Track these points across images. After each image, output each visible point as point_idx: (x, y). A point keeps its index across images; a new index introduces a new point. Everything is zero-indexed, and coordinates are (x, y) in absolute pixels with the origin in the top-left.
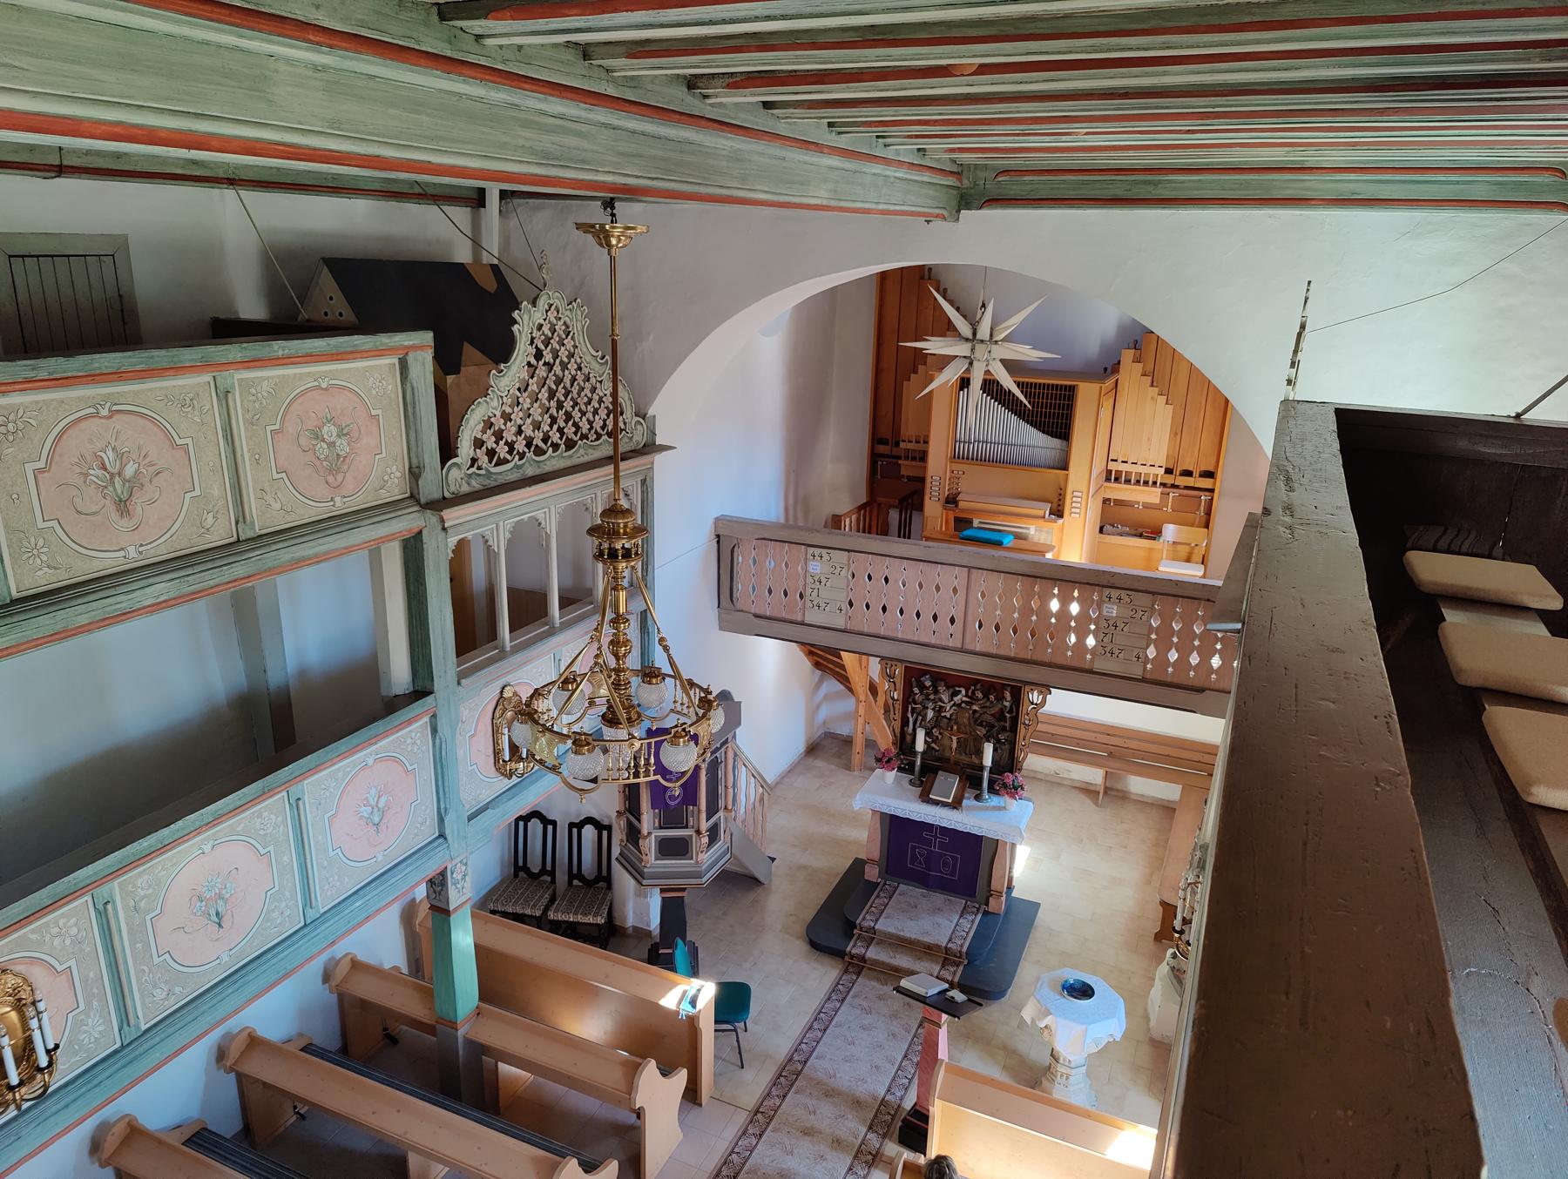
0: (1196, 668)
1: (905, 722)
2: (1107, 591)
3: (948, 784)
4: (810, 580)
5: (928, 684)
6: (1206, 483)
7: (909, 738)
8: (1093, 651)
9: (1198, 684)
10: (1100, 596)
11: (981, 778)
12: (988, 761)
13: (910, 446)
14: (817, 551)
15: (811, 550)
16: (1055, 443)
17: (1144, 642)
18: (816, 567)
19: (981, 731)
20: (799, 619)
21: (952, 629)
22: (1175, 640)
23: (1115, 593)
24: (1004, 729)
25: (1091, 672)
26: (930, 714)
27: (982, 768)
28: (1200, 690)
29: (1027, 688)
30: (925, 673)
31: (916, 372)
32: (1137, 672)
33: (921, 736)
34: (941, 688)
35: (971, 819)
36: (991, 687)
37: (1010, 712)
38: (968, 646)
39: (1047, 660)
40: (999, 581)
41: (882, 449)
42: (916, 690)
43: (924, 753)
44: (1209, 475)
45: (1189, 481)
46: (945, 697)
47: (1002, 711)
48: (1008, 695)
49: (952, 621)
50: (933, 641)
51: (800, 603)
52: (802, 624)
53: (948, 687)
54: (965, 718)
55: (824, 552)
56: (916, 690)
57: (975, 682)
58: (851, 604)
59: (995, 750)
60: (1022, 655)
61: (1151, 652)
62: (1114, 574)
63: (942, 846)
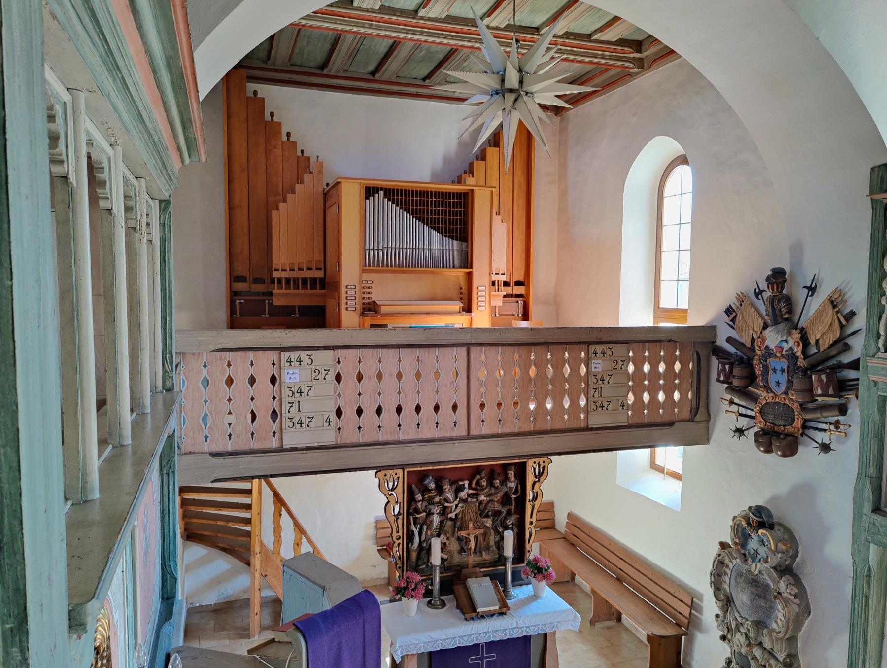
0: (664, 405)
2: (593, 348)
3: (481, 589)
4: (286, 392)
6: (520, 290)
8: (587, 411)
9: (666, 419)
10: (587, 354)
11: (505, 574)
13: (284, 275)
14: (294, 355)
15: (285, 355)
16: (457, 245)
17: (626, 389)
19: (489, 522)
21: (454, 418)
23: (599, 348)
24: (509, 513)
25: (587, 429)
26: (436, 519)
28: (671, 424)
30: (423, 475)
31: (285, 201)
32: (622, 420)
34: (447, 487)
36: (497, 473)
37: (516, 493)
38: (474, 432)
39: (547, 427)
40: (497, 355)
41: (240, 286)
42: (419, 497)
44: (519, 283)
45: (509, 290)
46: (450, 496)
48: (511, 474)
49: (455, 407)
50: (437, 434)
51: (275, 427)
52: (281, 450)
54: (472, 511)
55: (303, 354)
56: (419, 497)
58: (339, 413)
61: (631, 398)
62: (600, 329)
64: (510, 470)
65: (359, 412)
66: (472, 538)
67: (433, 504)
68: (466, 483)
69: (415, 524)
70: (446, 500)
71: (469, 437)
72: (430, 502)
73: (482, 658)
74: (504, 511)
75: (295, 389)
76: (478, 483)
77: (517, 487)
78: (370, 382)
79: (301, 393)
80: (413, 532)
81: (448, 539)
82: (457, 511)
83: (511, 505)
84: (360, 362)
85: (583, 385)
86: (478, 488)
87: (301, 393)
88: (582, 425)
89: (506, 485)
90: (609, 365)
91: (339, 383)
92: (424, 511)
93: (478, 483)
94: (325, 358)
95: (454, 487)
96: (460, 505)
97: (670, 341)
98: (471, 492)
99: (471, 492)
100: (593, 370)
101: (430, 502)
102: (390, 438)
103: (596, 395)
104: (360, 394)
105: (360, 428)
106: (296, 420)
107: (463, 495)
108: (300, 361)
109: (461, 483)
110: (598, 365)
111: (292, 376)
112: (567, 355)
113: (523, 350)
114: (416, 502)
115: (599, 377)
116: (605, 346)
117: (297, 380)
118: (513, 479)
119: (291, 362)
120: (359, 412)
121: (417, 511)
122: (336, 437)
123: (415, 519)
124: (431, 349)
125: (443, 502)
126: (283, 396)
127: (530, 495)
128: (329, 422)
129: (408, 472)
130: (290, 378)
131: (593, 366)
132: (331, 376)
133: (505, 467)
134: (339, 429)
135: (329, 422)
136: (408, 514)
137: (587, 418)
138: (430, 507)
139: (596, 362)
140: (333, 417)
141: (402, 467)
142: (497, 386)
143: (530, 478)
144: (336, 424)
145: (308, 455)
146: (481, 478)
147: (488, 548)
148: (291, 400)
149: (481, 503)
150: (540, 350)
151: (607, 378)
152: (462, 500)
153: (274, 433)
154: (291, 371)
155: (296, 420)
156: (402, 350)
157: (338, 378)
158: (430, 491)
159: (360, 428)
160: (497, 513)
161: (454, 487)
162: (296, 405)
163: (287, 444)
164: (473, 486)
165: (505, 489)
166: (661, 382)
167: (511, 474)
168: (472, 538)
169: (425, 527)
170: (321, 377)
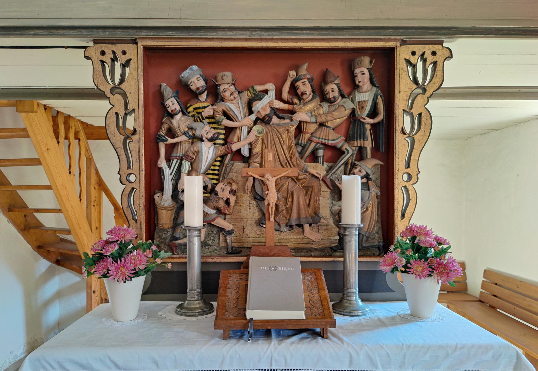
1: (154, 181)
7: (165, 218)
19: (319, 169)
24: (361, 155)
26: (208, 152)
27: (343, 232)
34: (227, 88)
37: (373, 114)
42: (172, 104)
46: (235, 106)
48: (363, 74)
56: (172, 104)
64: (360, 66)
68: (271, 87)
69: (169, 160)
74: (350, 150)
76: (293, 89)
80: (161, 171)
93: (293, 89)
96: (256, 128)
98: (278, 104)
99: (278, 104)
109: (259, 88)
114: (172, 115)
125: (219, 116)
138: (195, 125)
143: (403, 87)
147: (315, 219)
158: (195, 95)
161: (246, 96)
164: (285, 95)
165: (349, 105)
167: (363, 74)
168: (271, 183)
169: (186, 165)
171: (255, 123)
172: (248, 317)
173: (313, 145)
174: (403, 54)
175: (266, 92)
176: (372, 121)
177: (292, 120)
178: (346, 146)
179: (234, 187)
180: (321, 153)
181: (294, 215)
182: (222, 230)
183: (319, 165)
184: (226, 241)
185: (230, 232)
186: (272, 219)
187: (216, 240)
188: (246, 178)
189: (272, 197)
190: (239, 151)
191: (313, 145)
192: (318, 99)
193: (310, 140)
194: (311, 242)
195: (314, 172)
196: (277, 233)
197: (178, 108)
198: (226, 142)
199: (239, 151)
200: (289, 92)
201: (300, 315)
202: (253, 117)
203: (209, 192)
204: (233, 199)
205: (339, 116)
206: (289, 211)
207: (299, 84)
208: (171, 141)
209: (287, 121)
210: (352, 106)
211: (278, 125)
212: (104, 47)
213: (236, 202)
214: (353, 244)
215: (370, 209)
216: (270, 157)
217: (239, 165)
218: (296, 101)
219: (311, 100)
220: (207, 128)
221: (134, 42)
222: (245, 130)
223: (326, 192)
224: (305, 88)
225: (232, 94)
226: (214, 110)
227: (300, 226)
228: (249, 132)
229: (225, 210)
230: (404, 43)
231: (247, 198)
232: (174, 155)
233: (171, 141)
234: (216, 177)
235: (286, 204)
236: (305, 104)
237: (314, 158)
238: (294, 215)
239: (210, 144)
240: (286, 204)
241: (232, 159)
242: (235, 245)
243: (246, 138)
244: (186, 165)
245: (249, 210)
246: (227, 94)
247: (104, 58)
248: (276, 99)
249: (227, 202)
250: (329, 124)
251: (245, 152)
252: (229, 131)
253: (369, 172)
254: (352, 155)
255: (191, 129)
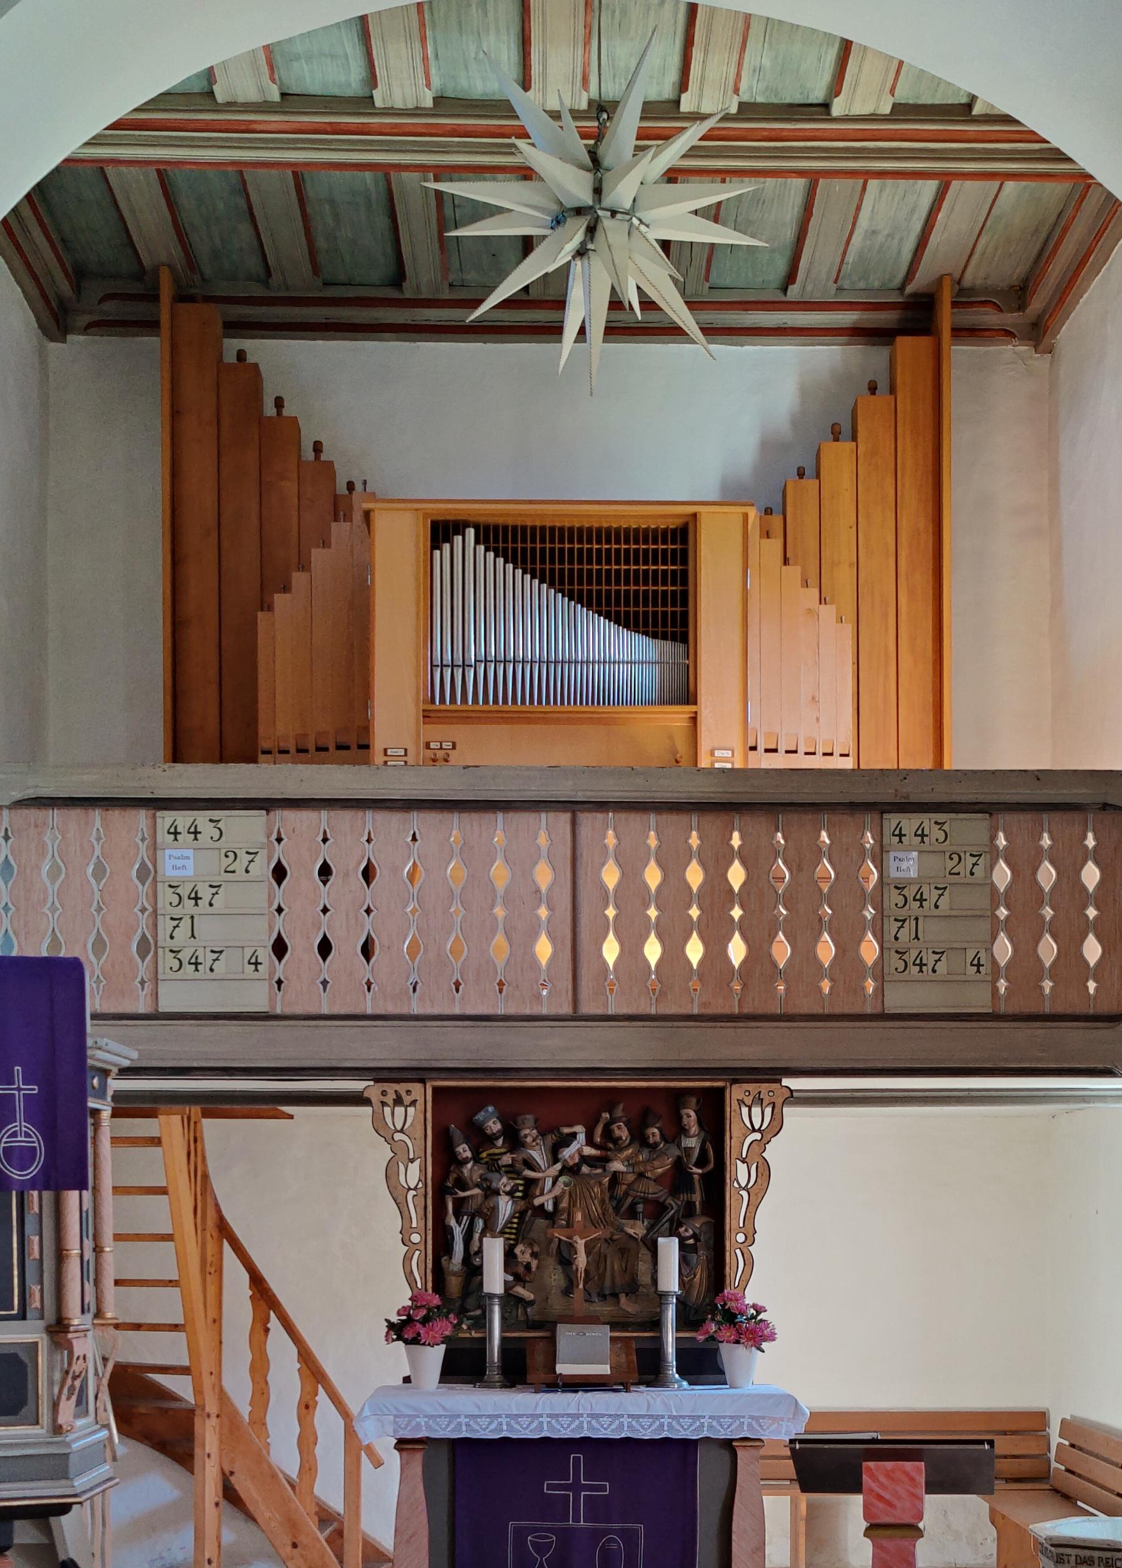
2: (892, 820)
3: (584, 1349)
4: (166, 897)
5: (494, 1126)
7: (454, 1284)
8: (880, 972)
10: (879, 838)
12: (670, 1280)
17: (986, 925)
18: (180, 863)
19: (637, 1229)
20: (142, 1008)
22: (1048, 912)
23: (910, 823)
24: (689, 1211)
26: (505, 1207)
29: (736, 1093)
32: (978, 1000)
33: (494, 1251)
34: (529, 1133)
35: (668, 1409)
37: (701, 1162)
42: (464, 1151)
43: (509, 1299)
46: (538, 1155)
47: (679, 1166)
48: (690, 1117)
52: (155, 1016)
53: (543, 1134)
56: (464, 1151)
57: (610, 1098)
58: (280, 948)
59: (684, 1261)
60: (719, 1007)
61: (1004, 949)
63: (596, 1509)
65: (325, 948)
66: (580, 1244)
67: (498, 1170)
68: (580, 1129)
69: (458, 1216)
70: (530, 1164)
71: (576, 1017)
72: (493, 1165)
73: (576, 1487)
74: (675, 1205)
75: (185, 891)
76: (608, 1133)
77: (703, 1151)
78: (348, 883)
79: (196, 898)
80: (450, 1231)
81: (534, 1255)
82: (557, 1191)
83: (693, 1191)
84: (325, 840)
85: (869, 912)
86: (608, 1144)
87: (196, 898)
88: (869, 1010)
89: (679, 1146)
90: (939, 865)
91: (279, 884)
92: (477, 1185)
93: (608, 1133)
94: (246, 827)
95: (551, 1139)
96: (562, 1179)
97: (1105, 807)
98: (589, 1151)
99: (589, 1151)
100: (894, 874)
101: (493, 1165)
102: (391, 1009)
103: (904, 935)
104: (325, 910)
105: (325, 983)
106: (185, 956)
107: (569, 1153)
108: (196, 833)
109: (566, 1130)
110: (908, 865)
111: (179, 863)
112: (824, 836)
113: (713, 822)
115: (910, 892)
116: (927, 820)
117: (190, 872)
118: (694, 1129)
119: (176, 833)
120: (325, 948)
121: (462, 1184)
122: (272, 1000)
123: (459, 1204)
124: (488, 817)
126: (160, 905)
127: (741, 1173)
128: (256, 964)
129: (436, 1090)
130: (174, 867)
131: (893, 865)
132: (262, 868)
133: (677, 1097)
134: (279, 982)
135: (256, 964)
136: (440, 1192)
137: (880, 991)
138: (490, 1175)
139: (900, 855)
140: (266, 955)
141: (418, 1074)
142: (648, 907)
144: (272, 972)
145: (209, 1030)
146: (613, 1121)
147: (633, 1288)
148: (177, 912)
149: (615, 1177)
150: (758, 824)
151: (931, 895)
152: (566, 1170)
153: (142, 982)
154: (177, 853)
155: (185, 956)
156: (417, 820)
157: (279, 873)
158: (490, 1139)
159: (325, 983)
160: (657, 1210)
161: (551, 1139)
162: (186, 924)
163: (165, 1006)
166: (1092, 913)
167: (690, 1117)
168: (580, 1244)
169: (480, 1224)
170: (239, 866)
171: (561, 1173)
172: (558, 1372)
173: (630, 1199)
174: (736, 1093)
175: (574, 1136)
176: (700, 1171)
177: (605, 1170)
178: (670, 1201)
179: (536, 1249)
180: (640, 1208)
181: (608, 1283)
182: (520, 1300)
183: (639, 1223)
184: (526, 1313)
185: (531, 1303)
186: (581, 1286)
187: (514, 1312)
188: (551, 1241)
189: (581, 1260)
190: (543, 1205)
191: (630, 1199)
192: (636, 1145)
193: (626, 1194)
194: (627, 1314)
195: (631, 1231)
196: (587, 1304)
197: (469, 1154)
198: (528, 1195)
199: (543, 1205)
200: (602, 1135)
201: (605, 1369)
202: (559, 1166)
203: (509, 1255)
204: (534, 1264)
205: (662, 1167)
206: (602, 1277)
207: (614, 1127)
208: (461, 1194)
209: (599, 1171)
210: (677, 1153)
211: (588, 1175)
212: (386, 1086)
213: (538, 1267)
214: (671, 1314)
215: (698, 1276)
216: (579, 1217)
217: (541, 1222)
218: (611, 1145)
219: (629, 1144)
220: (504, 1180)
221: (423, 1081)
222: (549, 1183)
223: (645, 1254)
224: (622, 1132)
225: (534, 1140)
226: (513, 1159)
227: (615, 1295)
228: (554, 1183)
229: (525, 1275)
230: (735, 1081)
231: (551, 1263)
232: (464, 1210)
233: (461, 1194)
234: (513, 1237)
235: (598, 1268)
236: (621, 1150)
237: (632, 1214)
238: (608, 1283)
239: (507, 1198)
240: (598, 1268)
241: (532, 1215)
242: (536, 1318)
243: (550, 1191)
244: (480, 1224)
245: (555, 1278)
246: (529, 1140)
247: (385, 1099)
248: (587, 1144)
249: (528, 1267)
250: (649, 1175)
251: (550, 1207)
252: (530, 1183)
253: (697, 1231)
254: (678, 1211)
255: (486, 1180)
